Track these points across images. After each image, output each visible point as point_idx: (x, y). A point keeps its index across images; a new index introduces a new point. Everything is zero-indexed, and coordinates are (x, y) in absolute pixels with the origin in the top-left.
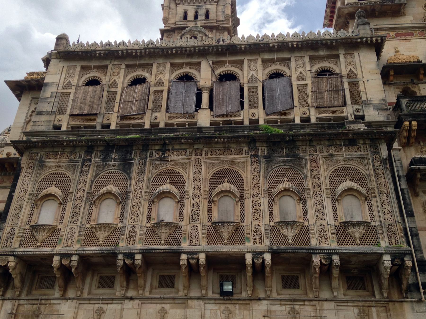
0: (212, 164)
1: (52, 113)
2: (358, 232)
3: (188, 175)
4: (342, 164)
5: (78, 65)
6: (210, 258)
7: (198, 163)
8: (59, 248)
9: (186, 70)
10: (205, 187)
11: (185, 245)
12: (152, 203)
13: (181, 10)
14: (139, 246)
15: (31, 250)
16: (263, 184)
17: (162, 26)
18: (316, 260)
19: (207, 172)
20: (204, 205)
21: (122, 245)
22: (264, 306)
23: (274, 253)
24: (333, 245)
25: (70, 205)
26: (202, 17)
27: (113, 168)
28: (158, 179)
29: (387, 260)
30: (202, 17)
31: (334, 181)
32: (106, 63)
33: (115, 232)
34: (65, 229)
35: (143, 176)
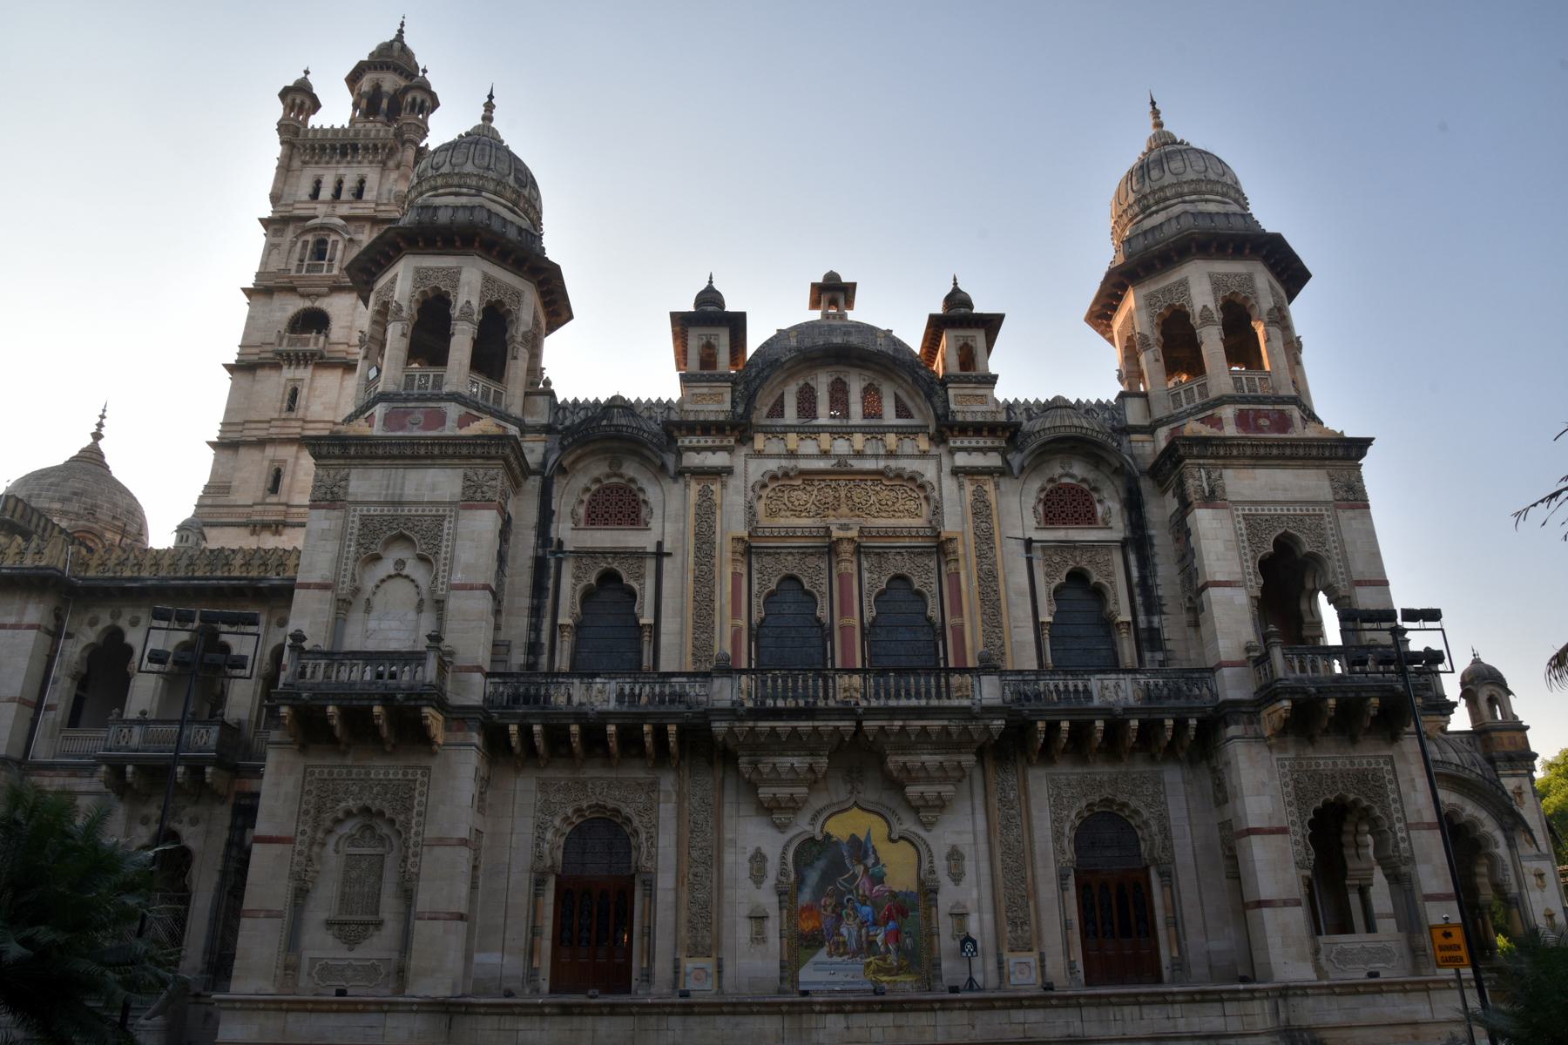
17: (267, 211)
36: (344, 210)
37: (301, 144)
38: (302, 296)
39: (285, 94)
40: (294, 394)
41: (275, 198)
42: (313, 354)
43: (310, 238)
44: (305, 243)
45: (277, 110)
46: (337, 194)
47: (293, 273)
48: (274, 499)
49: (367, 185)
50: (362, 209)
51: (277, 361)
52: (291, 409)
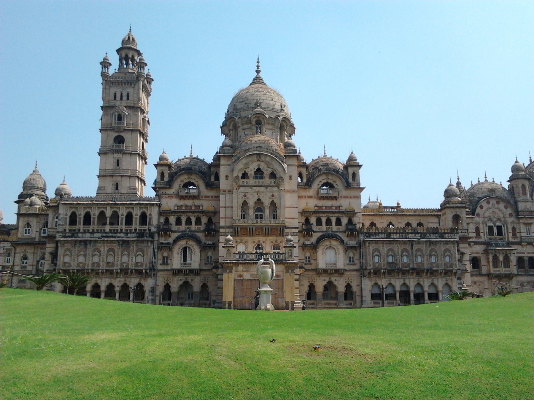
0: (108, 247)
1: (62, 225)
2: (139, 264)
3: (102, 249)
4: (139, 247)
5: (69, 206)
6: (106, 270)
7: (104, 246)
8: (71, 268)
9: (103, 209)
10: (106, 253)
11: (101, 268)
12: (92, 257)
13: (112, 90)
14: (90, 268)
15: (64, 268)
16: (120, 253)
18: (129, 271)
19: (106, 249)
20: (105, 257)
21: (86, 267)
22: (118, 279)
23: (120, 270)
24: (134, 268)
25: (72, 257)
26: (125, 98)
27: (82, 247)
28: (94, 251)
29: (144, 271)
30: (125, 98)
31: (137, 252)
32: (77, 206)
33: (84, 265)
34: (72, 264)
35: (90, 249)
36: (124, 103)
37: (108, 81)
38: (116, 132)
39: (101, 63)
40: (118, 160)
41: (103, 99)
42: (123, 150)
43: (117, 114)
44: (115, 115)
45: (99, 69)
46: (121, 98)
47: (113, 125)
48: (117, 191)
49: (130, 95)
50: (130, 103)
51: (114, 152)
52: (118, 165)
